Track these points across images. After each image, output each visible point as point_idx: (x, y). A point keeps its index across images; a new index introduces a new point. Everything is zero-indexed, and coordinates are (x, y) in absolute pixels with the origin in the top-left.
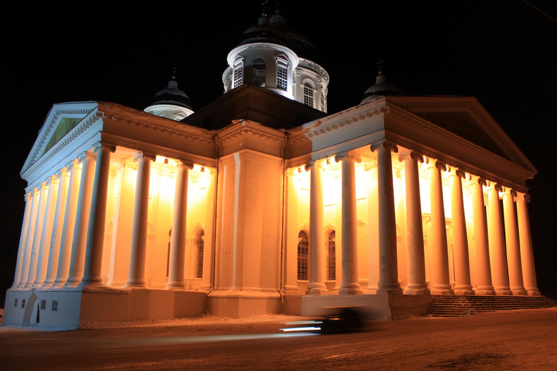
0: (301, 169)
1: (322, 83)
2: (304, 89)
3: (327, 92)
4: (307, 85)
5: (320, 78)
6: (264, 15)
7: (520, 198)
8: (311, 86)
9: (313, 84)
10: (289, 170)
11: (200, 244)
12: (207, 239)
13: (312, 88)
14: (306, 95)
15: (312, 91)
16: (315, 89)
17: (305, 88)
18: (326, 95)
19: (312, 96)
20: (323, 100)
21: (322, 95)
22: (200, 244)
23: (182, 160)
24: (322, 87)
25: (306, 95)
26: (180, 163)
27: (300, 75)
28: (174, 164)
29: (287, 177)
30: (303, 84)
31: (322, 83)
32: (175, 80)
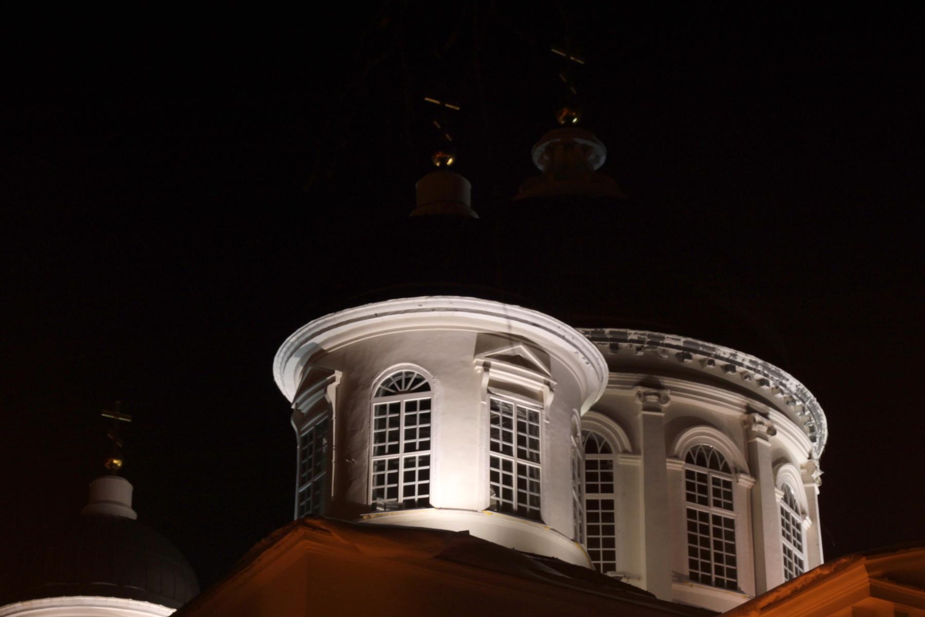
1: (781, 438)
2: (684, 479)
3: (817, 474)
5: (765, 415)
6: (443, 162)
8: (722, 458)
9: (731, 451)
13: (726, 469)
14: (699, 508)
15: (728, 484)
16: (743, 472)
17: (689, 474)
18: (809, 492)
20: (798, 519)
21: (789, 499)
24: (781, 459)
25: (699, 508)
30: (676, 457)
31: (781, 438)
32: (121, 473)
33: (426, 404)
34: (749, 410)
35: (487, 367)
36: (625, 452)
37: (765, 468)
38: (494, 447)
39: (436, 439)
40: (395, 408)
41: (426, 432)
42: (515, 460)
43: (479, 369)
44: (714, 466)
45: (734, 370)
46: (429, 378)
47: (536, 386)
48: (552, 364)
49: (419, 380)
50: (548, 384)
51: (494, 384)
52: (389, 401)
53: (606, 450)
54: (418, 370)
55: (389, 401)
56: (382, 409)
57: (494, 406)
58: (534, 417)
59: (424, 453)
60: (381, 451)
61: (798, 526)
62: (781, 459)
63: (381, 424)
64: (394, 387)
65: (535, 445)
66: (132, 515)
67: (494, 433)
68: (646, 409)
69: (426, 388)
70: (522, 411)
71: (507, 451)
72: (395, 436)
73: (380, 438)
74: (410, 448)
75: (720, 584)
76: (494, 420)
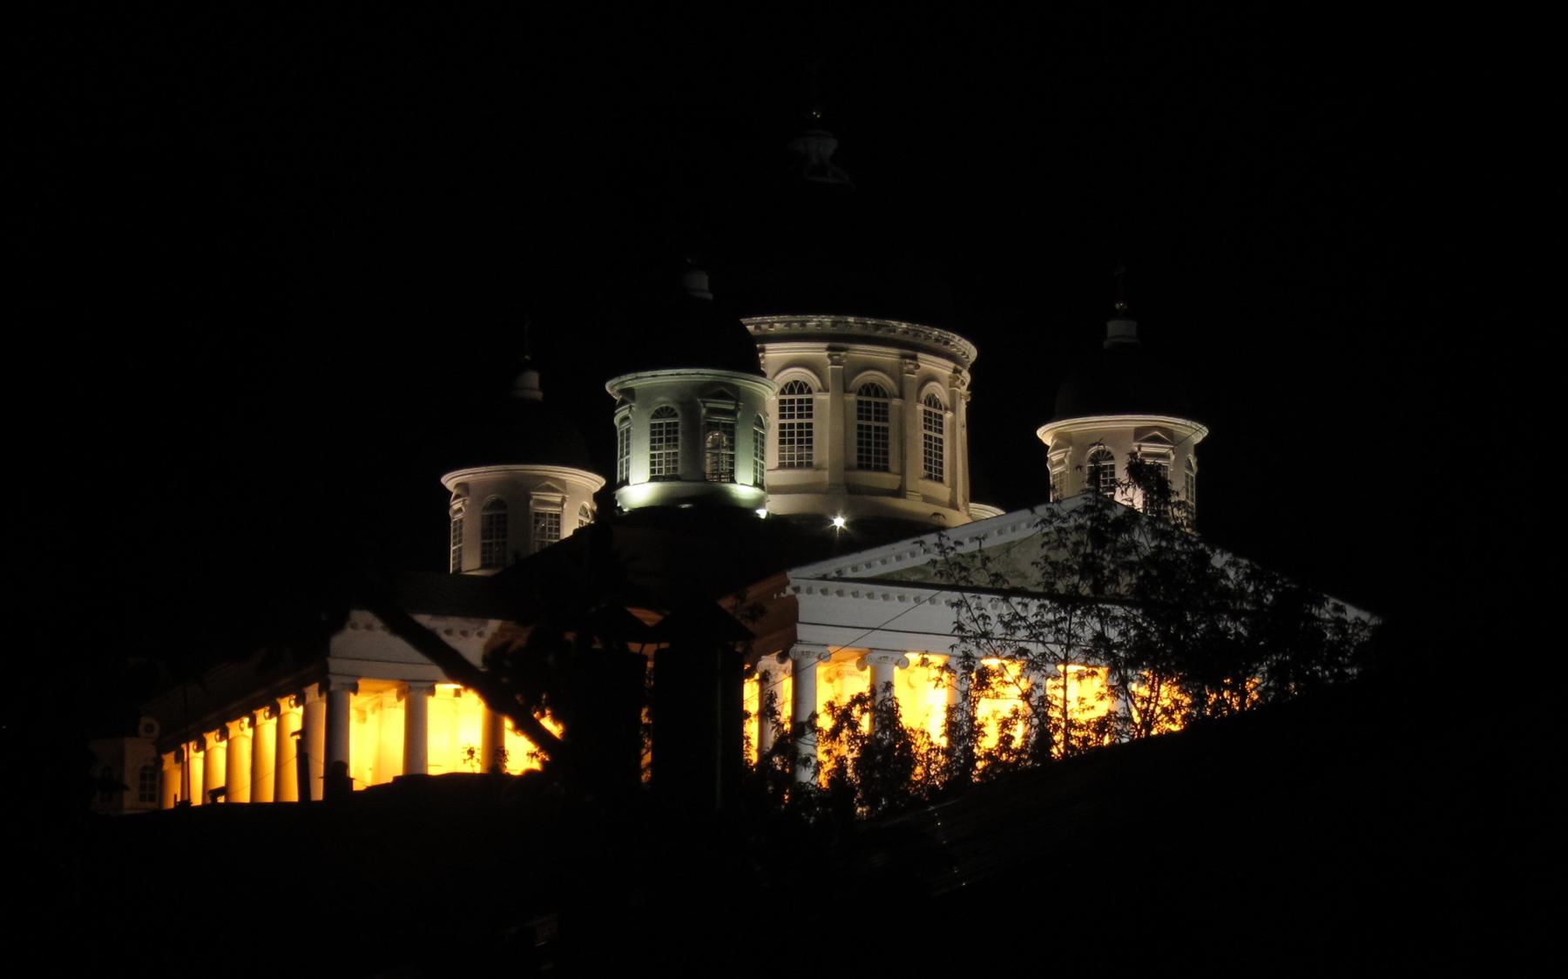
2: (856, 406)
4: (871, 389)
13: (885, 396)
14: (864, 423)
16: (896, 397)
27: (841, 367)
35: (704, 403)
36: (819, 391)
37: (910, 390)
44: (877, 395)
53: (810, 391)
66: (539, 395)
68: (832, 364)
75: (877, 469)
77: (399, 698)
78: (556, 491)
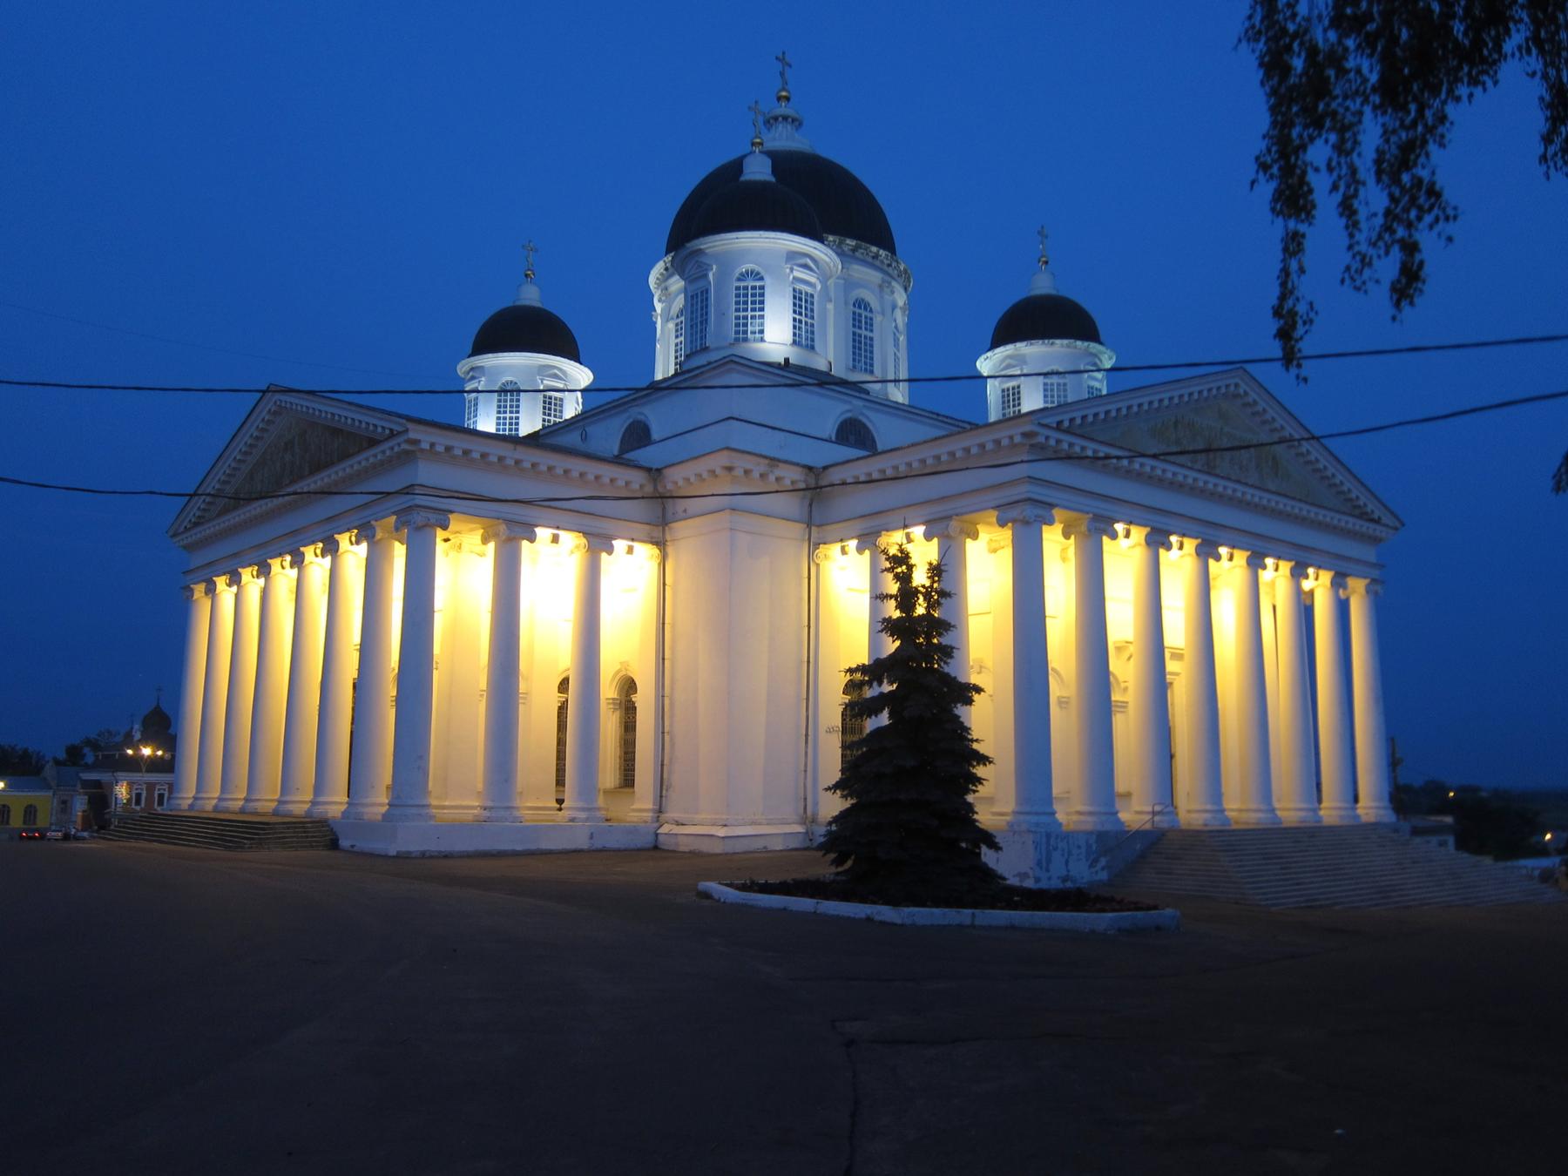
0: (846, 548)
4: (861, 304)
7: (1357, 591)
9: (874, 303)
10: (823, 549)
11: (628, 710)
12: (644, 700)
14: (858, 331)
18: (903, 321)
19: (872, 331)
21: (896, 327)
22: (628, 710)
23: (585, 534)
25: (858, 331)
26: (583, 541)
28: (572, 541)
29: (818, 565)
33: (762, 288)
34: (883, 281)
35: (792, 270)
38: (795, 312)
39: (767, 306)
40: (746, 288)
41: (762, 302)
42: (804, 319)
43: (788, 270)
44: (865, 309)
45: (877, 258)
46: (763, 273)
47: (813, 280)
48: (820, 265)
49: (758, 274)
50: (818, 278)
51: (794, 278)
52: (742, 284)
54: (757, 268)
55: (742, 284)
56: (738, 288)
57: (794, 290)
58: (812, 296)
59: (761, 313)
60: (737, 310)
61: (899, 340)
62: (894, 307)
63: (738, 296)
64: (743, 277)
65: (812, 310)
67: (795, 305)
69: (762, 279)
70: (806, 293)
71: (800, 314)
72: (746, 303)
73: (737, 303)
74: (753, 310)
76: (795, 297)
77: (485, 541)
78: (560, 379)
